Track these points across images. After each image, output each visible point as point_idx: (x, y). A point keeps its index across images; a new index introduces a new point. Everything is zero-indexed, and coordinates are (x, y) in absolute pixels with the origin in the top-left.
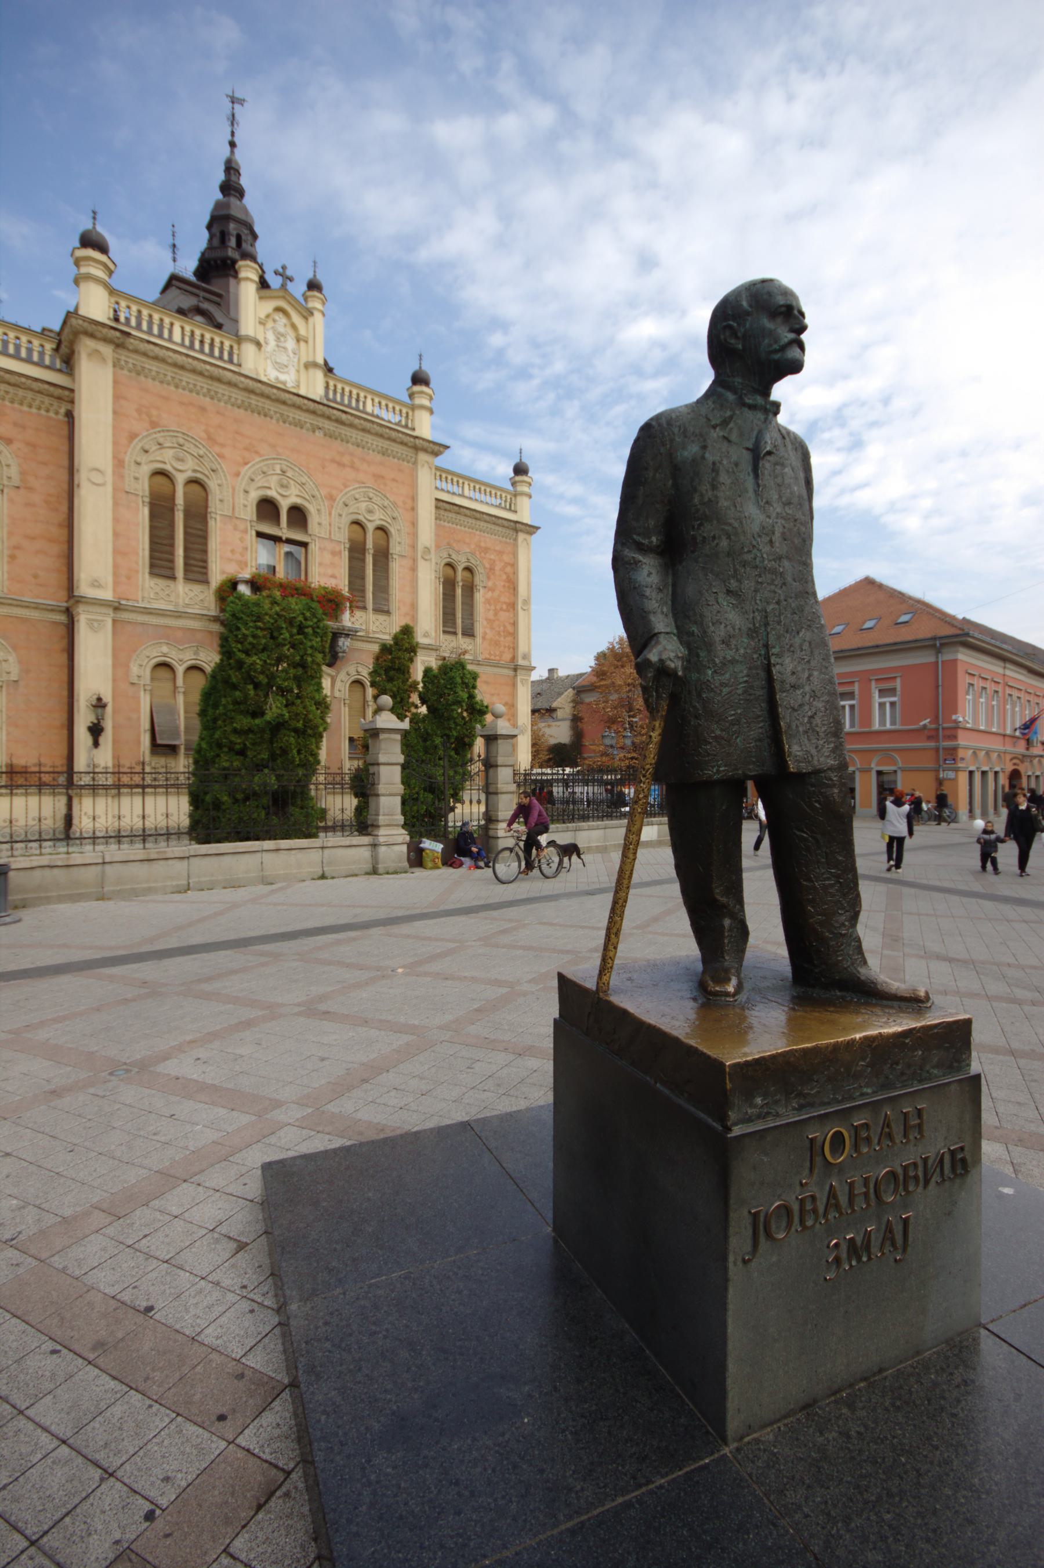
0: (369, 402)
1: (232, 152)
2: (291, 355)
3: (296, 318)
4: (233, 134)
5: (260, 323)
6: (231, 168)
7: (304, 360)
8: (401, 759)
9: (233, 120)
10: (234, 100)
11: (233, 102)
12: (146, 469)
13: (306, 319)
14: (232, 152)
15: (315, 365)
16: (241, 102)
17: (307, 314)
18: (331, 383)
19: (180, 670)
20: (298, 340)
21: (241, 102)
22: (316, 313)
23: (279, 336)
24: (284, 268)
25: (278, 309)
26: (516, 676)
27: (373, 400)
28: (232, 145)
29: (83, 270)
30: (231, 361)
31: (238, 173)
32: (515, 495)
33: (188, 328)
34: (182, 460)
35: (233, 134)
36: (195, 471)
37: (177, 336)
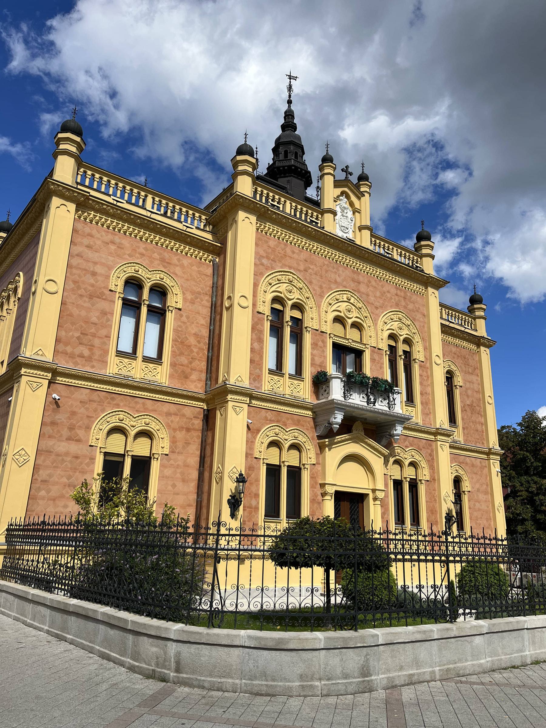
1: (289, 106)
2: (350, 222)
3: (353, 198)
4: (290, 96)
5: (335, 201)
6: (289, 115)
7: (358, 225)
10: (290, 77)
11: (290, 79)
13: (359, 198)
14: (289, 106)
16: (295, 78)
17: (360, 195)
20: (354, 213)
21: (295, 78)
22: (365, 194)
23: (343, 209)
24: (347, 167)
26: (489, 459)
27: (397, 250)
28: (290, 102)
29: (240, 168)
31: (293, 117)
32: (475, 319)
35: (290, 96)
36: (298, 299)
37: (288, 210)
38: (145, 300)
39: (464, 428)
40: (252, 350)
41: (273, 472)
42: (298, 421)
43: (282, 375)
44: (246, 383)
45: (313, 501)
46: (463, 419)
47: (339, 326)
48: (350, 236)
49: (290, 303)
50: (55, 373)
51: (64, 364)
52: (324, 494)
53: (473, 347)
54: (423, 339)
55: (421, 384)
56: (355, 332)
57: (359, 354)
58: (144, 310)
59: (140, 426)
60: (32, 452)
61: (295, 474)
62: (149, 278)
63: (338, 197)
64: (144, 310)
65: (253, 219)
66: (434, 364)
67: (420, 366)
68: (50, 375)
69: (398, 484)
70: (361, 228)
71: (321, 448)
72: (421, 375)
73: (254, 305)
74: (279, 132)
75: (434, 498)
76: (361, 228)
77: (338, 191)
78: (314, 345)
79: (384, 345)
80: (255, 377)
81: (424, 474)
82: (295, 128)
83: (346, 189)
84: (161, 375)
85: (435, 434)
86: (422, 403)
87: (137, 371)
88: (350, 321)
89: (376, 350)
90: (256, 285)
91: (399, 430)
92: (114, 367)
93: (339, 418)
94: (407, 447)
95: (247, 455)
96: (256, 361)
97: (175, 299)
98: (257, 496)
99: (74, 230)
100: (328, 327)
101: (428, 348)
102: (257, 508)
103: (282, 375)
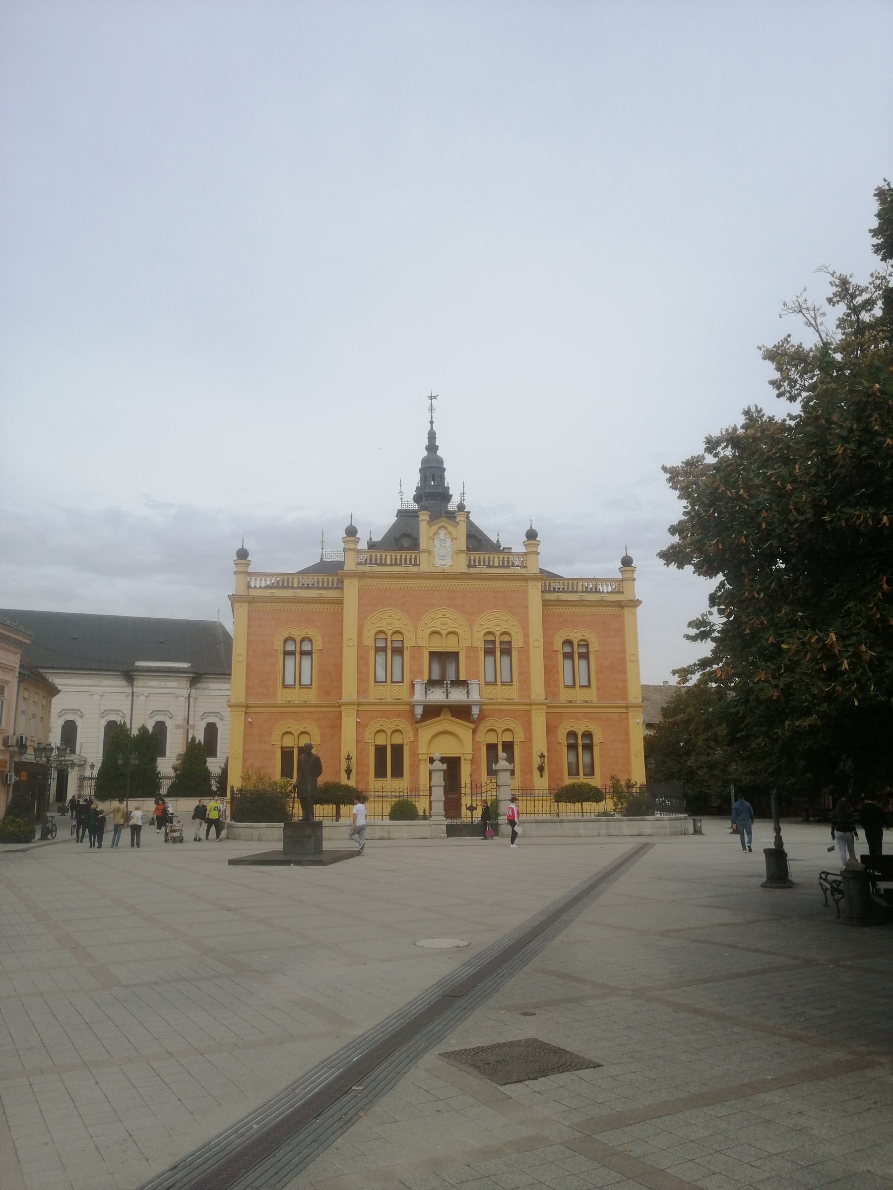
0: (496, 560)
2: (448, 549)
3: (450, 528)
8: (443, 783)
9: (432, 409)
10: (431, 398)
12: (374, 631)
15: (461, 552)
16: (435, 397)
18: (472, 557)
19: (389, 733)
21: (435, 397)
25: (440, 528)
28: (432, 422)
30: (416, 565)
33: (394, 555)
34: (390, 624)
37: (388, 562)
38: (298, 651)
39: (598, 688)
40: (359, 672)
41: (380, 751)
42: (399, 714)
43: (386, 685)
44: (354, 697)
45: (411, 766)
46: (597, 680)
47: (436, 637)
48: (447, 562)
49: (389, 633)
50: (247, 707)
51: (251, 702)
52: (419, 761)
53: (616, 611)
54: (523, 628)
55: (519, 666)
56: (453, 638)
57: (457, 654)
58: (298, 655)
59: (301, 729)
60: (240, 751)
61: (398, 750)
62: (298, 634)
63: (435, 533)
64: (298, 655)
65: (355, 582)
66: (531, 648)
67: (519, 652)
68: (244, 709)
69: (492, 748)
70: (457, 552)
71: (416, 732)
72: (519, 659)
73: (360, 641)
74: (425, 453)
75: (528, 754)
76: (457, 552)
77: (435, 528)
78: (412, 658)
79: (480, 644)
80: (362, 689)
81: (519, 737)
82: (436, 448)
83: (442, 524)
84: (311, 696)
85: (530, 705)
86: (519, 681)
87: (295, 696)
88: (444, 633)
89: (472, 649)
90: (360, 628)
91: (475, 711)
92: (283, 696)
93: (419, 711)
94: (500, 718)
95: (358, 742)
96: (362, 680)
97: (318, 644)
98: (368, 766)
99: (249, 619)
100: (423, 643)
101: (526, 636)
102: (368, 773)
103: (386, 685)
